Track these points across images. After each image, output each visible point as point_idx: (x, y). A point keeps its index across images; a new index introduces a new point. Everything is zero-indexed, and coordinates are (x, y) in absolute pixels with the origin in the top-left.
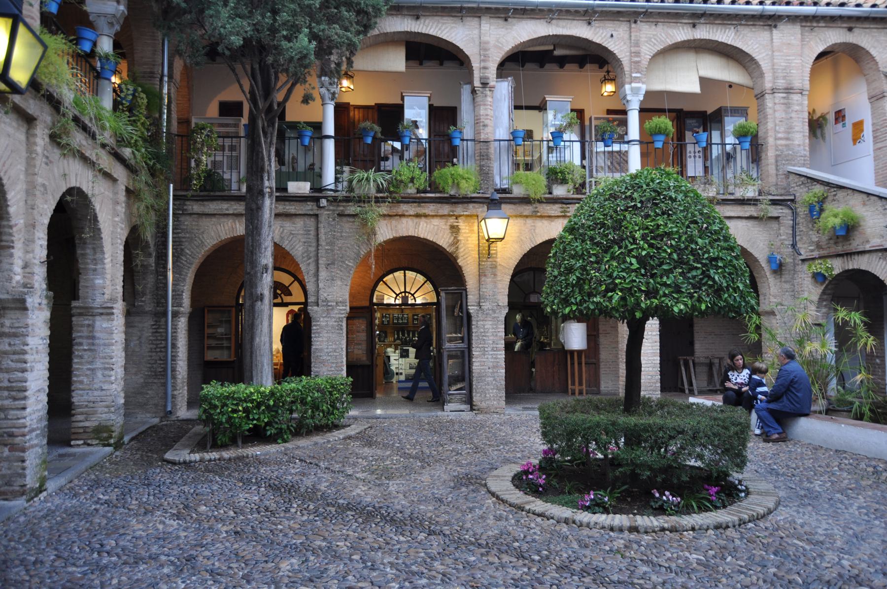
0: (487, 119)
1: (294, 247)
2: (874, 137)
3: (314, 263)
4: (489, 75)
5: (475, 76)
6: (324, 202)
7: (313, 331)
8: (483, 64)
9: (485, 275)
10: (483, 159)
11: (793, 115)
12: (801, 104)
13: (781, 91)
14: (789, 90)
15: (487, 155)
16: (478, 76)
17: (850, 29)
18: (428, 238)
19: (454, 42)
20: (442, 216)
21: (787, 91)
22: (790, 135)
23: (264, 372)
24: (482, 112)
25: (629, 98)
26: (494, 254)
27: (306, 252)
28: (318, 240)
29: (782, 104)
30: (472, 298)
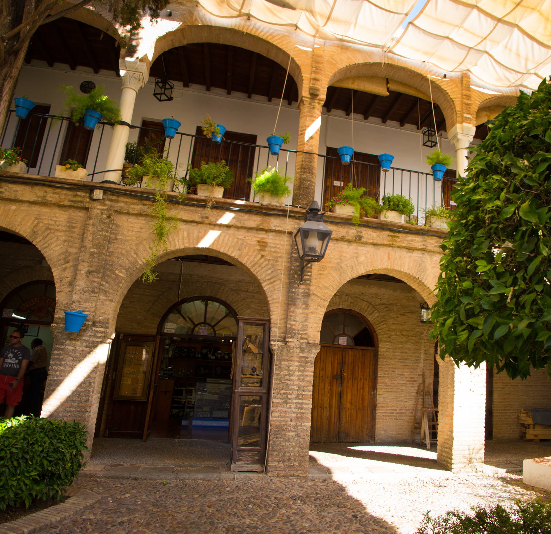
1: (49, 245)
3: (72, 269)
4: (319, 87)
5: (304, 85)
6: (98, 194)
8: (313, 76)
9: (295, 305)
10: (304, 172)
15: (309, 168)
16: (308, 86)
18: (229, 253)
19: (285, 50)
20: (250, 229)
26: (308, 280)
27: (63, 253)
28: (83, 241)
30: (276, 332)
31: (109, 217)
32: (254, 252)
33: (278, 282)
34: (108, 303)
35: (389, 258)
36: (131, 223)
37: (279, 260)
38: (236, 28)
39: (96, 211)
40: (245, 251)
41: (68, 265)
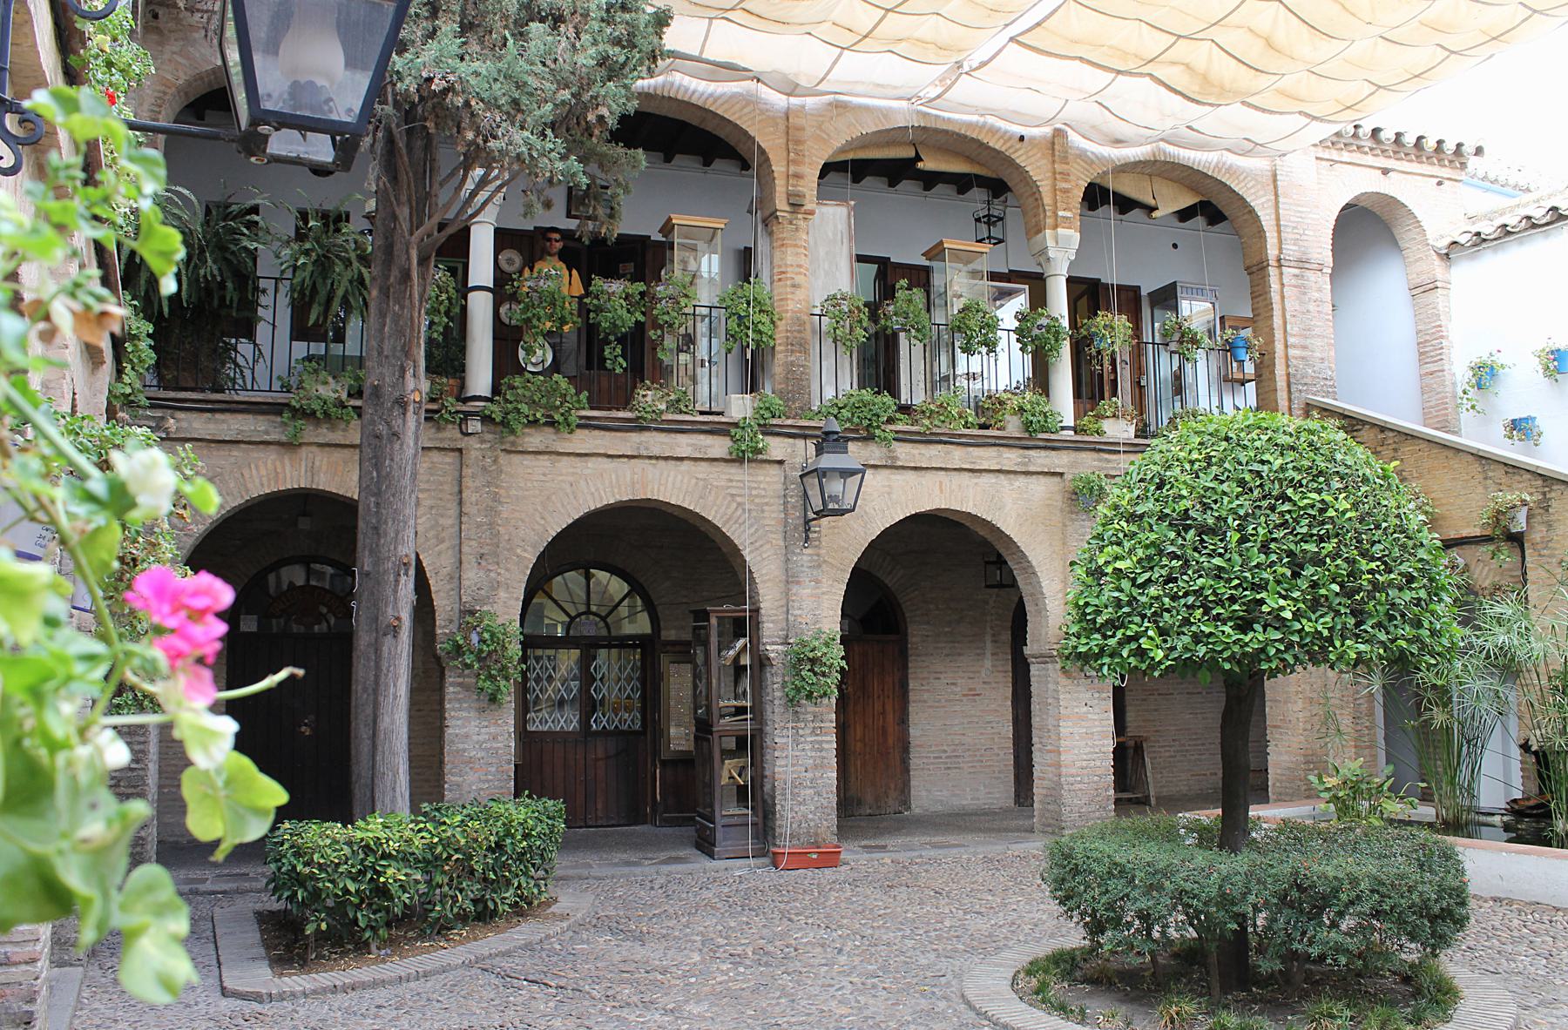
0: (800, 273)
2: (1421, 354)
6: (474, 426)
7: (447, 697)
8: (792, 169)
9: (798, 583)
10: (792, 351)
11: (1312, 307)
12: (1320, 290)
13: (1292, 264)
14: (1302, 263)
17: (1385, 171)
21: (1301, 265)
22: (1309, 341)
23: (398, 789)
24: (790, 259)
25: (1051, 254)
27: (432, 528)
28: (460, 503)
29: (1295, 286)
31: (495, 461)
32: (724, 498)
33: (768, 546)
34: (512, 602)
35: (941, 491)
36: (527, 467)
37: (766, 508)
38: (651, 91)
39: (474, 454)
40: (711, 498)
41: (443, 546)
